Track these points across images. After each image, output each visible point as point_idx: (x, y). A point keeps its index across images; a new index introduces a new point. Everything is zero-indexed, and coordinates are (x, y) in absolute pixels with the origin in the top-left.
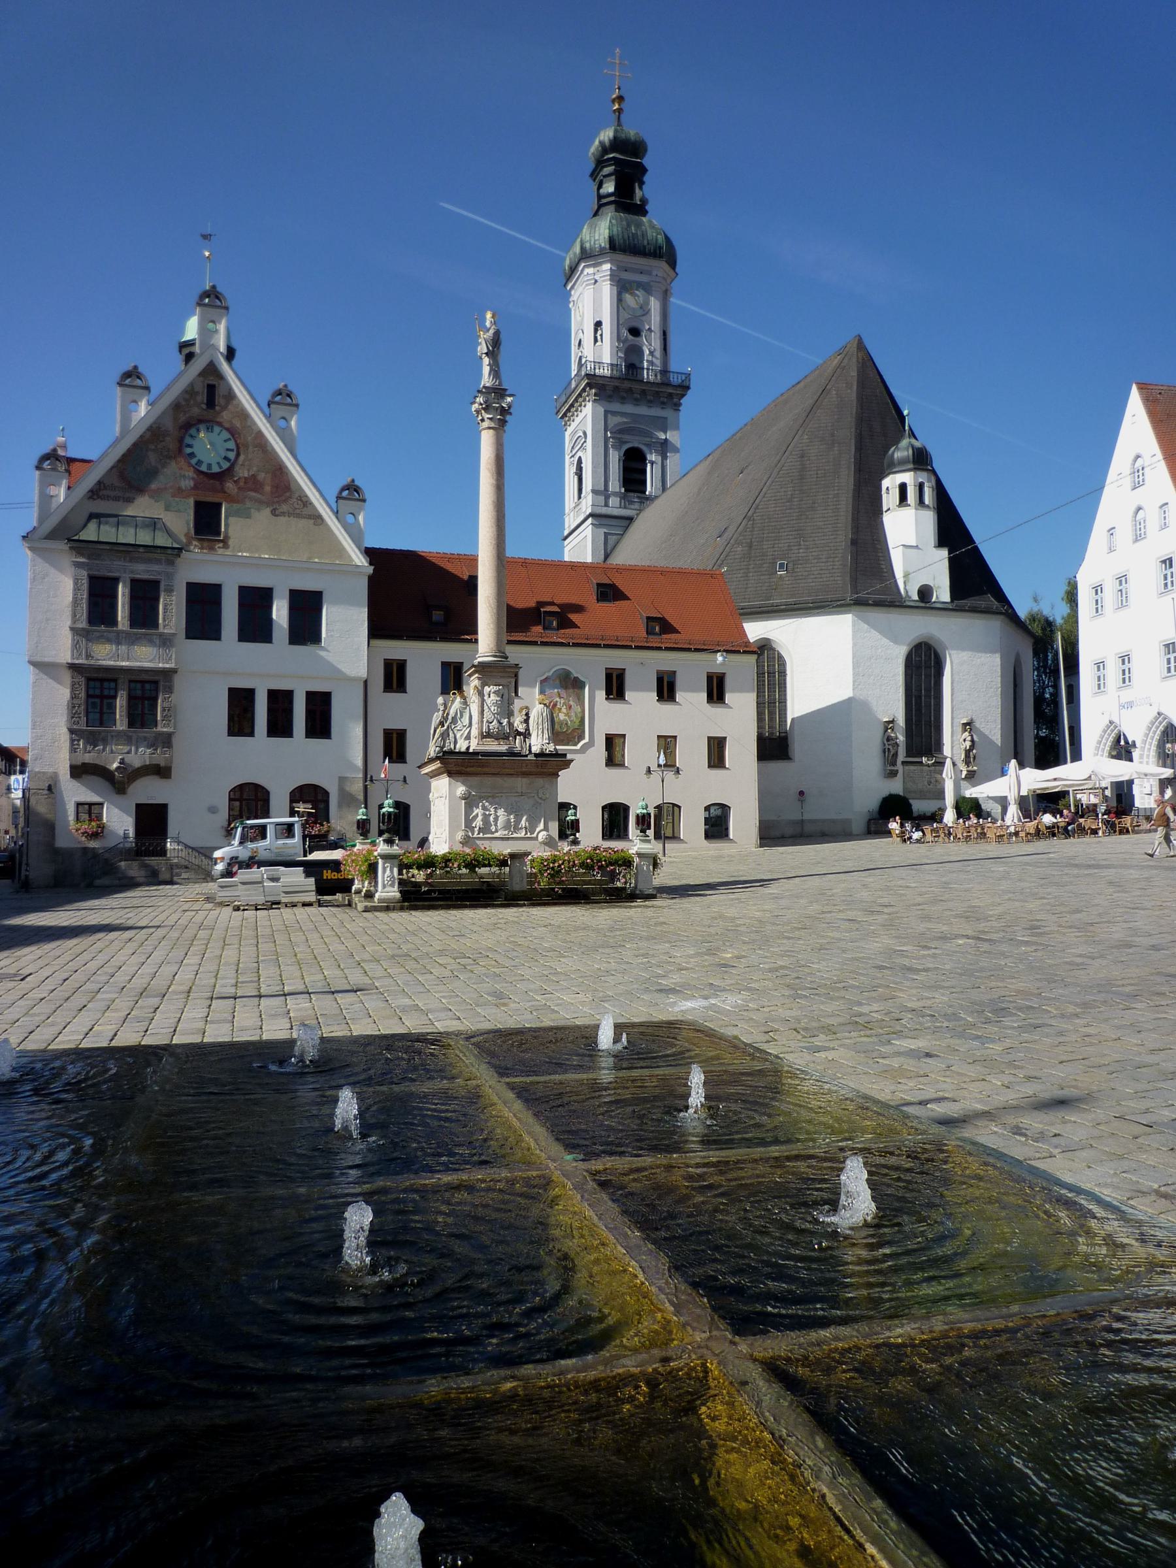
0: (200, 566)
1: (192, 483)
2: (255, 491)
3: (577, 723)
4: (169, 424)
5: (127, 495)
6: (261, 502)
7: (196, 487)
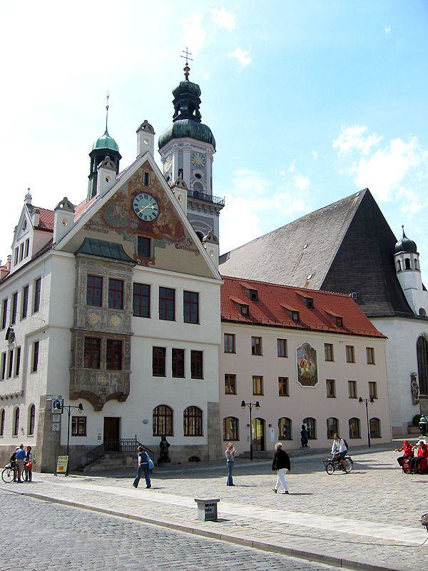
0: (141, 275)
2: (167, 233)
4: (126, 192)
5: (105, 229)
6: (170, 240)
7: (138, 228)
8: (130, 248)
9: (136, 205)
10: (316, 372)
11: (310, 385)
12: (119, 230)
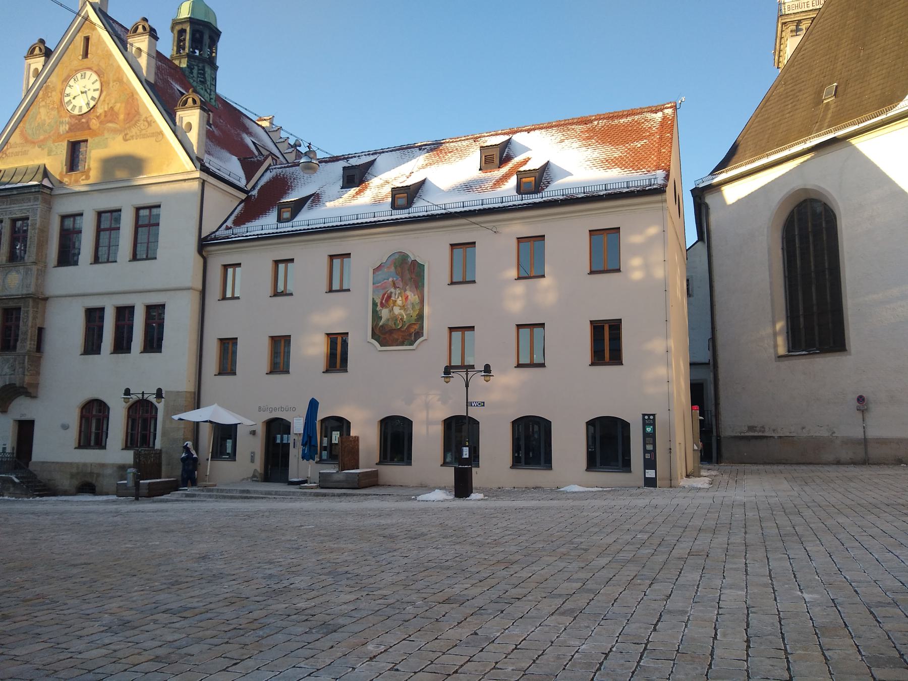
1: (67, 127)
2: (110, 122)
3: (414, 317)
7: (70, 130)
10: (420, 317)
11: (402, 344)
12: (41, 144)
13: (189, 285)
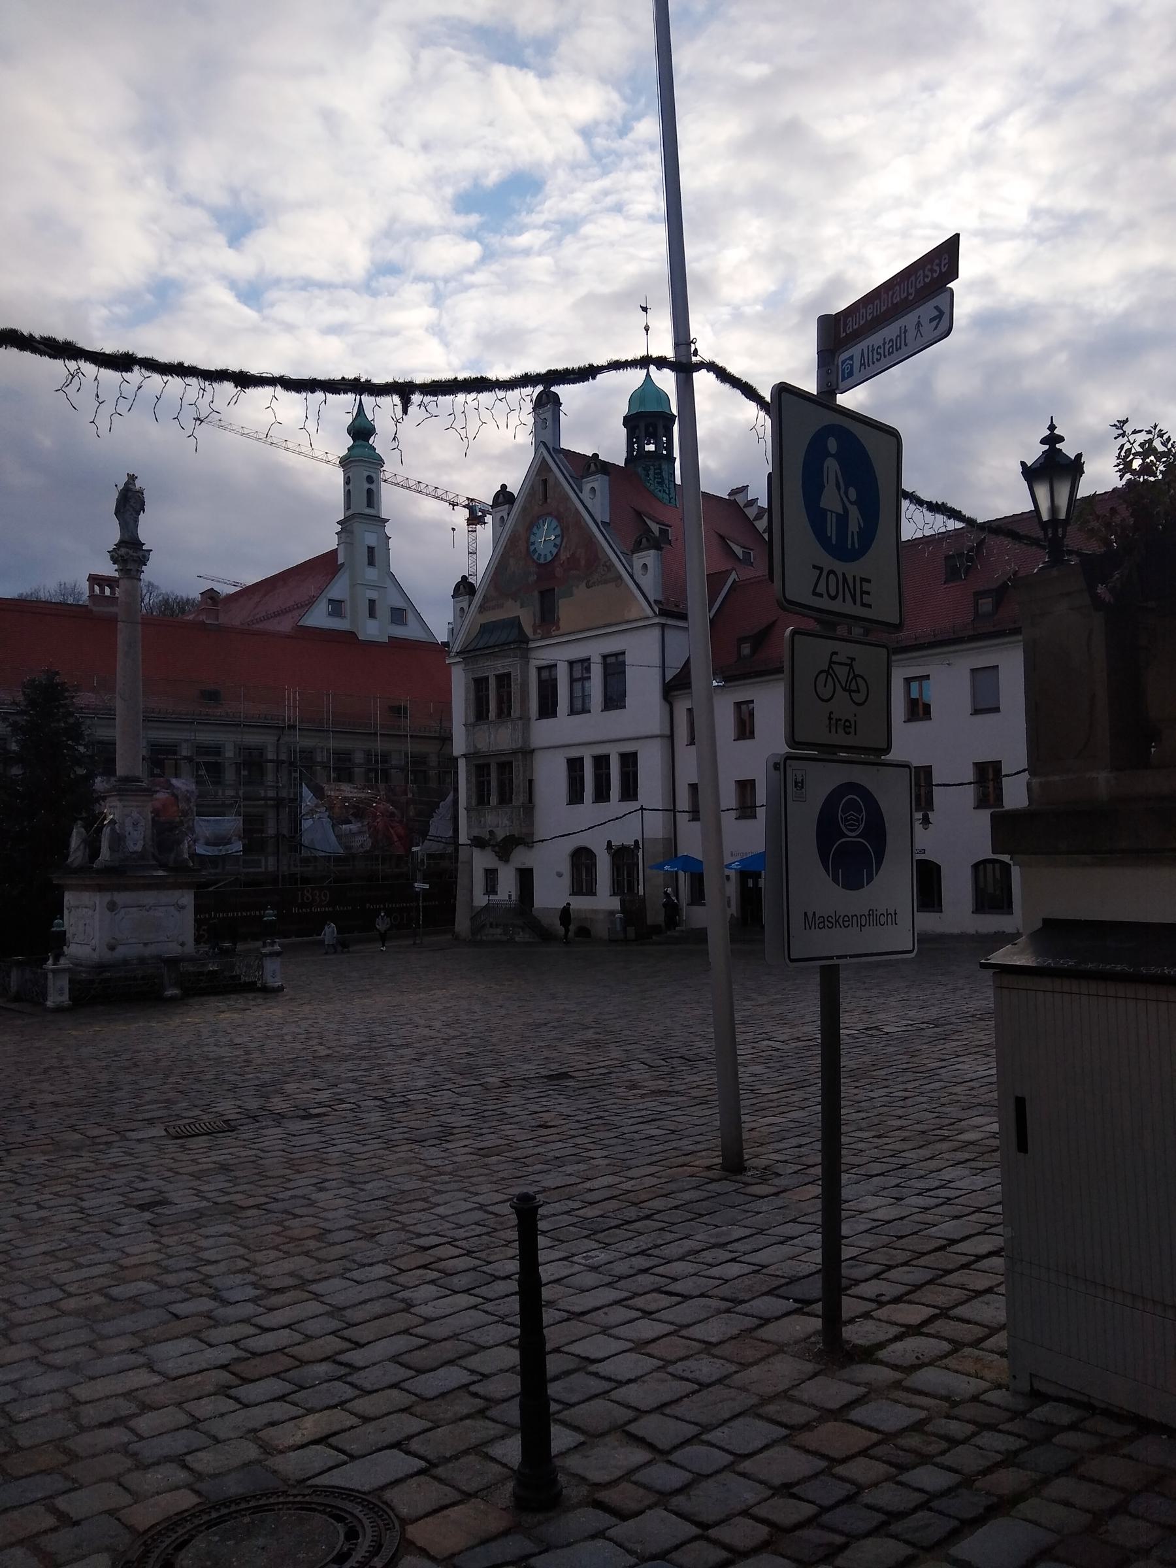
8: (527, 618)
9: (533, 543)
13: (658, 732)
